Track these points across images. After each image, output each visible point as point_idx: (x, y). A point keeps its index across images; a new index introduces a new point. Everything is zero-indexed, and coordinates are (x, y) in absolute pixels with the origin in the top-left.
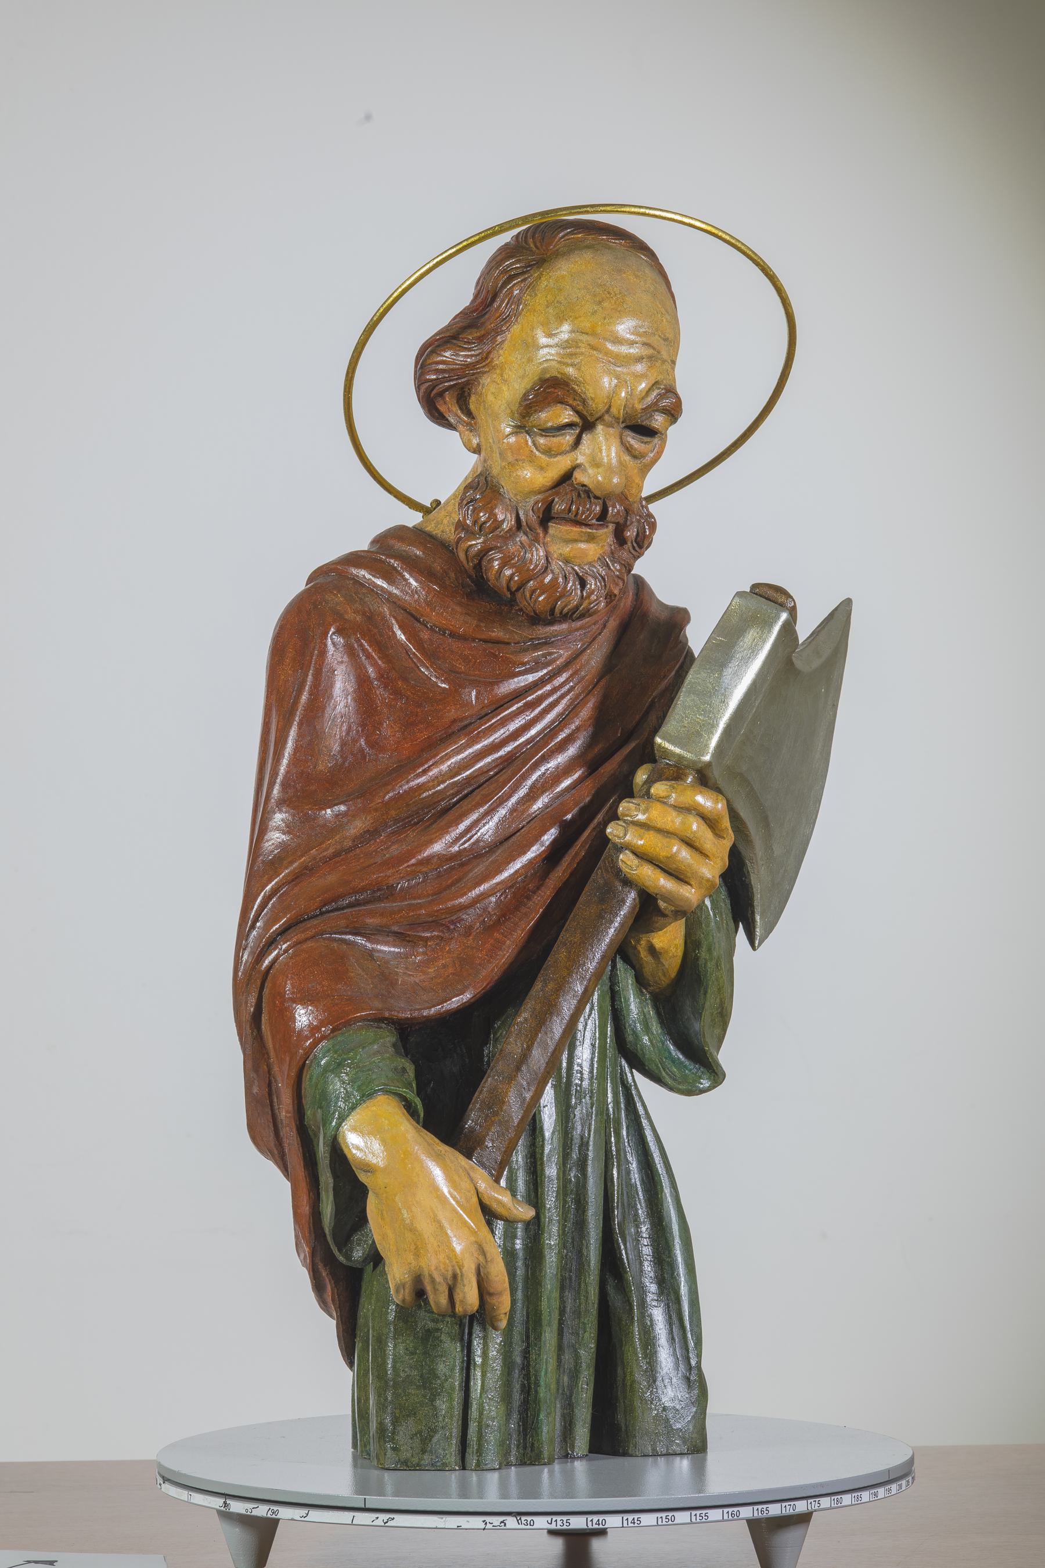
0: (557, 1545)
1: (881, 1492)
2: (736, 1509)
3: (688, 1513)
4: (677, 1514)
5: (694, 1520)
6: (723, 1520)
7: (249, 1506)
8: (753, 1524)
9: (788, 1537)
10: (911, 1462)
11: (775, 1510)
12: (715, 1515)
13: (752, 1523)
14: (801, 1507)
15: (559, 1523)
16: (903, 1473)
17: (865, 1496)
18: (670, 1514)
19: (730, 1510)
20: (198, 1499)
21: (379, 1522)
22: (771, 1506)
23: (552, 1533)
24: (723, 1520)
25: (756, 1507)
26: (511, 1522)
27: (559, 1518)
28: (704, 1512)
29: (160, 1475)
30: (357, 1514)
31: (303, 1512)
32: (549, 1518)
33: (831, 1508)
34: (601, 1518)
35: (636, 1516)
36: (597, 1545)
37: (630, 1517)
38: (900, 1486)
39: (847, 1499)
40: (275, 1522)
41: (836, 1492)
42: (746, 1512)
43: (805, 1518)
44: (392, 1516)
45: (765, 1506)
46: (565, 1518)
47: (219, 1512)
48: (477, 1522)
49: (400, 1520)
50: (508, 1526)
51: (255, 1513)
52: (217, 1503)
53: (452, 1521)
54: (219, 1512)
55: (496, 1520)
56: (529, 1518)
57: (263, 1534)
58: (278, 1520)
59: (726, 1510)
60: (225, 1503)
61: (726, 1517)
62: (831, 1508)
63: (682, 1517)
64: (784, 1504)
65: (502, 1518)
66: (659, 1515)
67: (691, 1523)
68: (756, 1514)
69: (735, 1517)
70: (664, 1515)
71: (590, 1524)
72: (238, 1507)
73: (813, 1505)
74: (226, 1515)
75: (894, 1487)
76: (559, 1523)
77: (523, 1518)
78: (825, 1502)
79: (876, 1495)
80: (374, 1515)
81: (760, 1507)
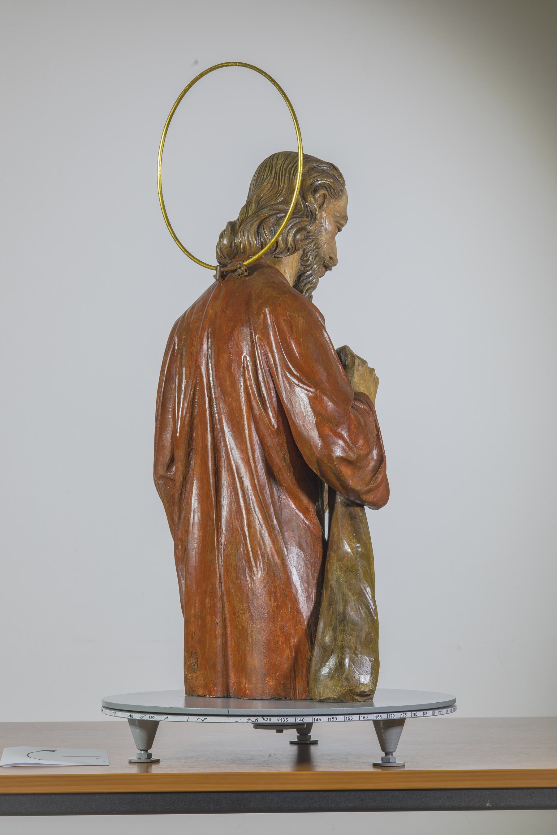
0: (295, 748)
2: (366, 715)
3: (342, 717)
4: (338, 717)
9: (393, 732)
10: (454, 701)
12: (356, 717)
13: (376, 723)
14: (397, 716)
15: (283, 720)
16: (449, 705)
22: (382, 715)
23: (292, 743)
24: (360, 720)
25: (375, 715)
27: (282, 718)
28: (350, 716)
30: (190, 717)
31: (165, 717)
33: (412, 717)
34: (302, 718)
35: (318, 717)
36: (313, 748)
37: (316, 718)
38: (447, 711)
39: (420, 714)
42: (371, 717)
44: (206, 717)
46: (285, 718)
47: (128, 719)
49: (210, 719)
50: (259, 722)
51: (144, 718)
53: (233, 719)
56: (269, 718)
57: (149, 730)
58: (156, 724)
59: (361, 716)
65: (256, 718)
66: (329, 717)
67: (345, 721)
69: (366, 719)
72: (136, 716)
73: (403, 715)
74: (132, 722)
77: (265, 718)
78: (409, 714)
80: (198, 717)
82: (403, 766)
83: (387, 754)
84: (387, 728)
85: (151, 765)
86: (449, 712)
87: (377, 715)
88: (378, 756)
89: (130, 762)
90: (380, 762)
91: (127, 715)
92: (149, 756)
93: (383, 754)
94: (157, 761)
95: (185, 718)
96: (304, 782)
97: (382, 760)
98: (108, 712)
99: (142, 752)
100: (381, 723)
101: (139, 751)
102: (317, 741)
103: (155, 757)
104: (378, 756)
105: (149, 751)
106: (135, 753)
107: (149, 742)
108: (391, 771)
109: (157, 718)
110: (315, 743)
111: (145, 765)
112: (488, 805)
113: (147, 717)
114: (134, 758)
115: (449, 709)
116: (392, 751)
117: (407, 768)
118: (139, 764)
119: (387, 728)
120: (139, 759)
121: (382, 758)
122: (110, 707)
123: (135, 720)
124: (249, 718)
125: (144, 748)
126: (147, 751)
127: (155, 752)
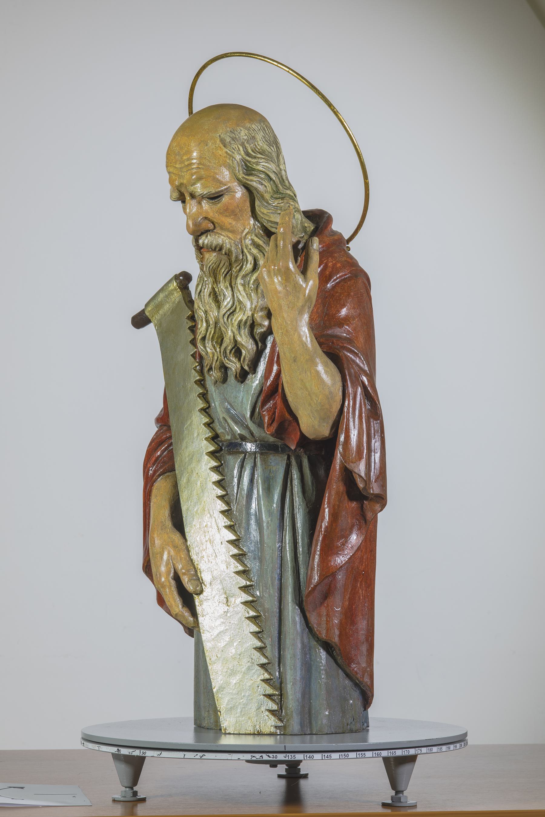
1: (452, 747)
7: (131, 750)
9: (405, 768)
14: (412, 752)
17: (444, 748)
22: (397, 751)
33: (427, 753)
39: (435, 749)
40: (142, 759)
41: (430, 744)
52: (114, 750)
54: (113, 754)
60: (118, 749)
62: (427, 753)
64: (403, 750)
73: (418, 751)
74: (116, 757)
78: (424, 750)
79: (449, 748)
81: (391, 751)
82: (415, 806)
83: (397, 792)
84: (398, 764)
85: (136, 805)
88: (387, 794)
90: (390, 801)
93: (393, 793)
94: (143, 800)
100: (392, 760)
108: (402, 812)
109: (149, 753)
111: (130, 804)
116: (403, 789)
122: (88, 739)
123: (121, 754)
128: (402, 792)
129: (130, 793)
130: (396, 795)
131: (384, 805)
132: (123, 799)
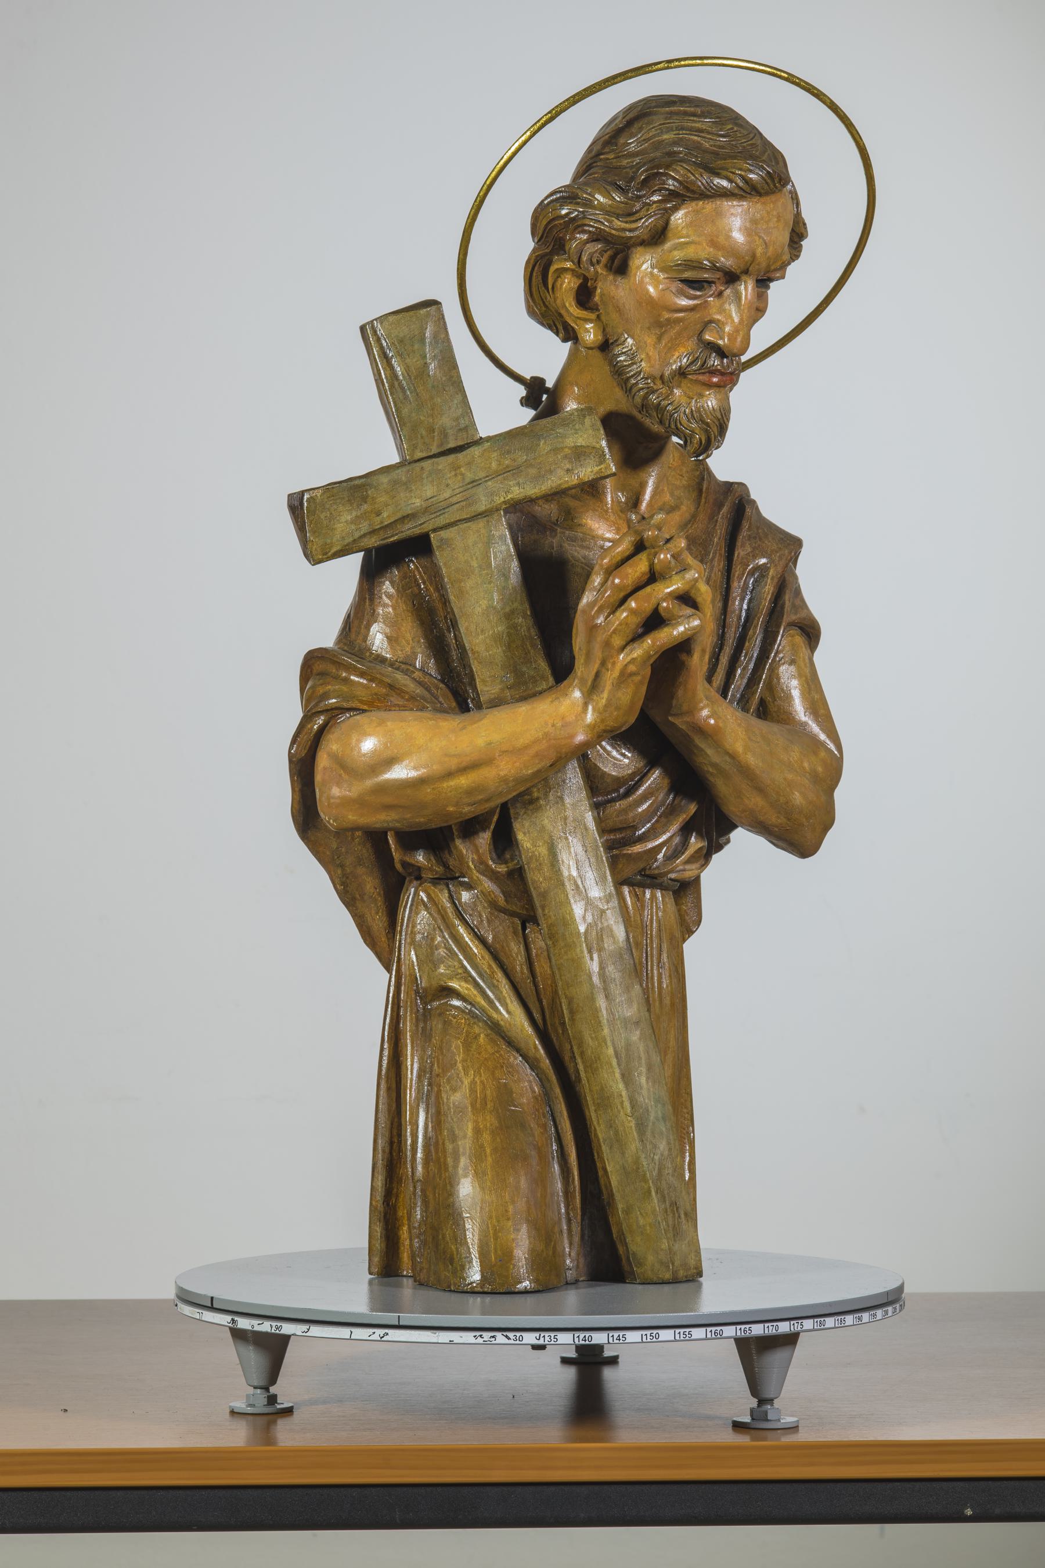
0: (570, 1373)
1: (866, 1316)
2: (719, 1328)
3: (672, 1331)
4: (661, 1332)
5: (677, 1338)
6: (706, 1339)
7: (255, 1322)
8: (742, 1344)
9: (776, 1357)
10: (900, 1289)
11: (757, 1330)
12: (698, 1333)
14: (784, 1327)
15: (547, 1339)
16: (892, 1299)
17: (849, 1319)
18: (655, 1332)
19: (713, 1329)
20: (209, 1316)
21: (376, 1337)
24: (706, 1339)
25: (738, 1327)
26: (500, 1338)
27: (547, 1334)
28: (688, 1330)
29: (179, 1297)
31: (305, 1327)
32: (537, 1334)
33: (814, 1330)
35: (621, 1333)
36: (608, 1373)
37: (616, 1334)
38: (886, 1312)
39: (830, 1322)
41: (819, 1313)
42: (729, 1331)
43: (791, 1339)
44: (390, 1331)
45: (748, 1326)
47: (230, 1328)
48: (468, 1337)
53: (444, 1337)
54: (230, 1328)
55: (487, 1335)
56: (518, 1334)
58: (286, 1339)
59: (709, 1329)
60: (233, 1320)
61: (709, 1336)
62: (814, 1330)
63: (666, 1335)
66: (644, 1332)
67: (675, 1340)
68: (739, 1333)
69: (719, 1336)
70: (648, 1332)
71: (576, 1340)
72: (244, 1323)
75: (879, 1313)
76: (547, 1339)
77: (511, 1335)
78: (808, 1324)
79: (860, 1319)
80: (371, 1331)
83: (762, 1402)
85: (275, 1422)
86: (890, 1314)
87: (743, 1327)
88: (743, 1407)
89: (233, 1413)
90: (747, 1419)
91: (225, 1319)
92: (272, 1400)
93: (754, 1402)
95: (344, 1332)
96: (589, 1462)
97: (752, 1415)
98: (187, 1310)
99: (259, 1391)
101: (251, 1391)
102: (617, 1357)
103: (284, 1403)
104: (743, 1407)
105: (273, 1390)
106: (242, 1394)
107: (273, 1374)
110: (613, 1361)
112: (969, 1512)
113: (266, 1327)
114: (240, 1405)
115: (890, 1309)
116: (772, 1396)
117: (804, 1436)
118: (250, 1418)
119: (762, 1350)
120: (250, 1405)
121: (752, 1411)
124: (478, 1334)
125: (262, 1384)
126: (267, 1389)
127: (286, 1390)
128: (770, 1401)
129: (261, 1398)
130: (759, 1406)
131: (737, 1426)
132: (249, 1410)
